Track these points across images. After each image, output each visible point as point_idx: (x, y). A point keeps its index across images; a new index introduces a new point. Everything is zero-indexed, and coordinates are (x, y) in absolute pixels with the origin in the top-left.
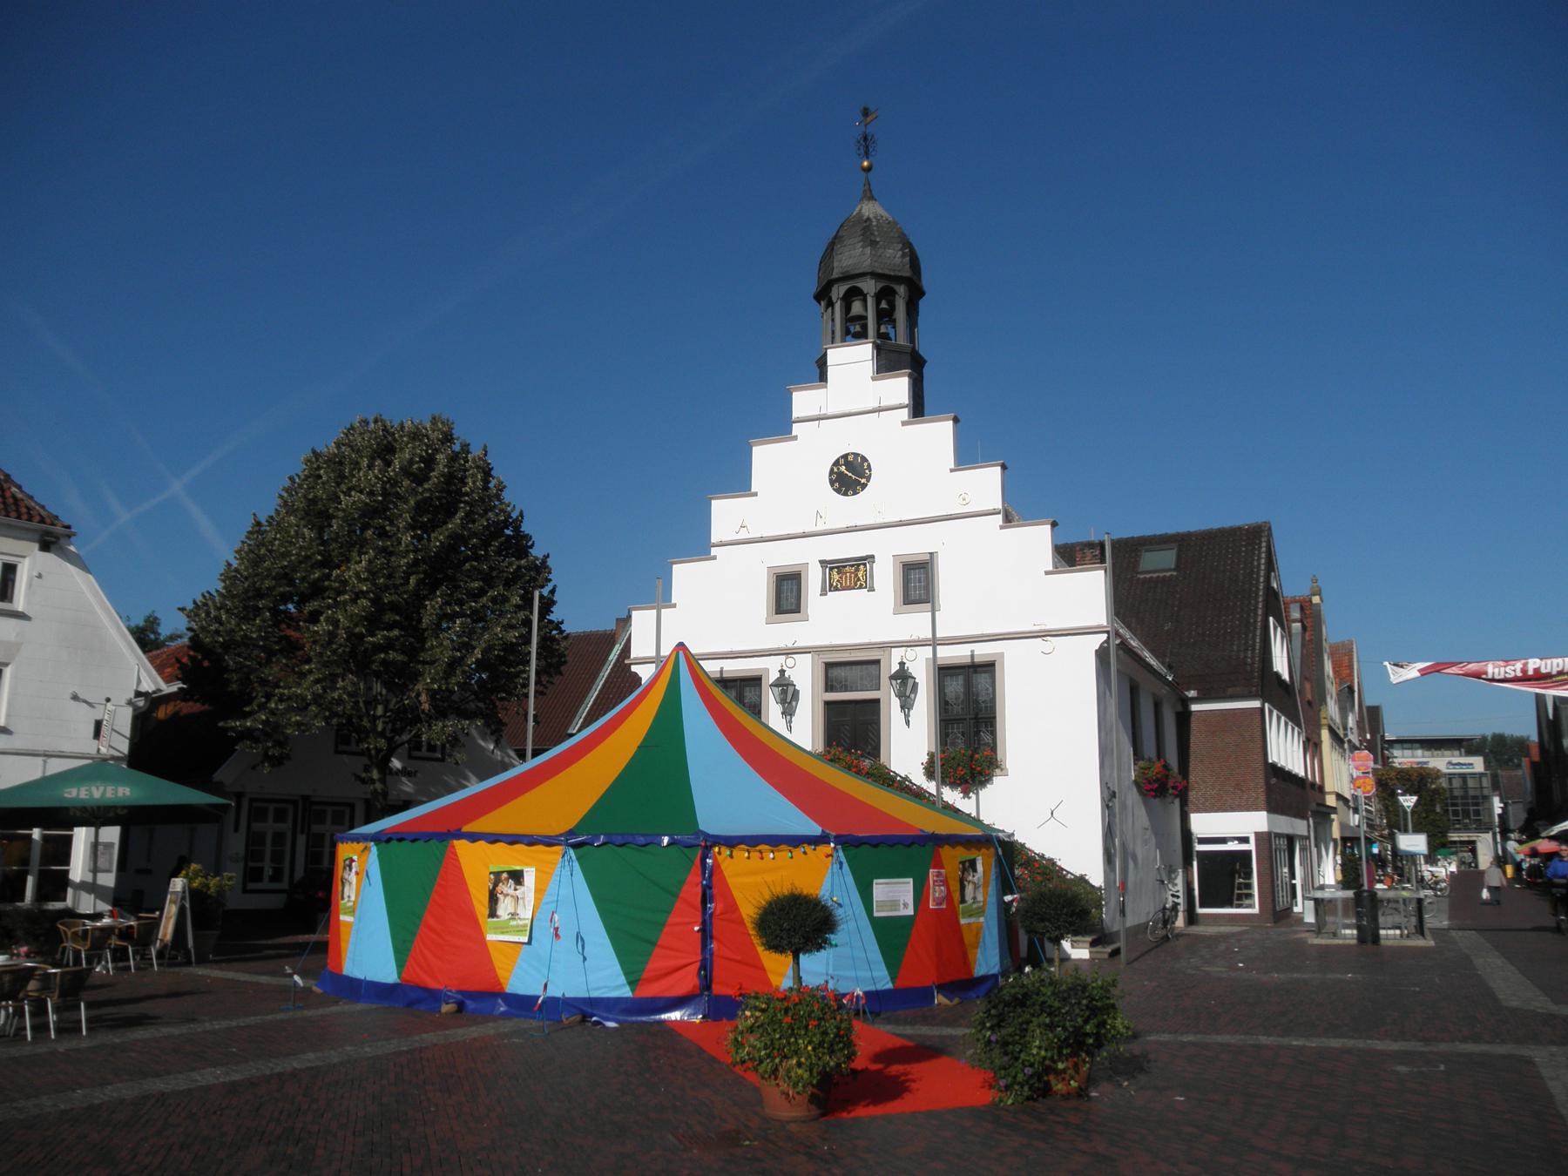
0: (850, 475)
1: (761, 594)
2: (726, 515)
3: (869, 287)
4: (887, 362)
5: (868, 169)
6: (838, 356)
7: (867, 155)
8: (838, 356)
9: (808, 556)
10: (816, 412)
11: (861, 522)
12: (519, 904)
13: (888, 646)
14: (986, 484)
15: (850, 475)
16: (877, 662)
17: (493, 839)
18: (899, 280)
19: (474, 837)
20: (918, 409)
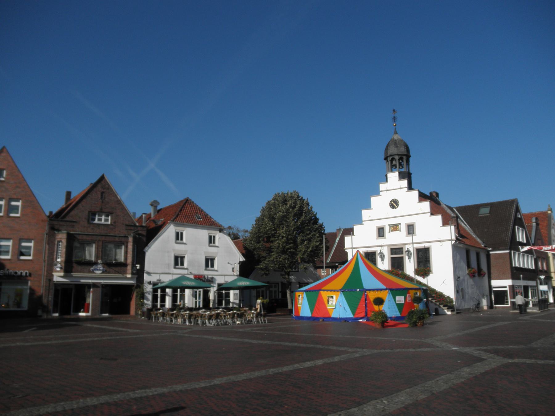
0: (394, 204)
1: (375, 233)
2: (366, 214)
3: (397, 157)
4: (402, 176)
5: (395, 126)
6: (390, 175)
7: (395, 122)
8: (390, 175)
9: (386, 224)
10: (385, 189)
12: (333, 302)
15: (394, 204)
16: (402, 248)
17: (327, 291)
18: (404, 155)
19: (324, 290)
20: (410, 188)
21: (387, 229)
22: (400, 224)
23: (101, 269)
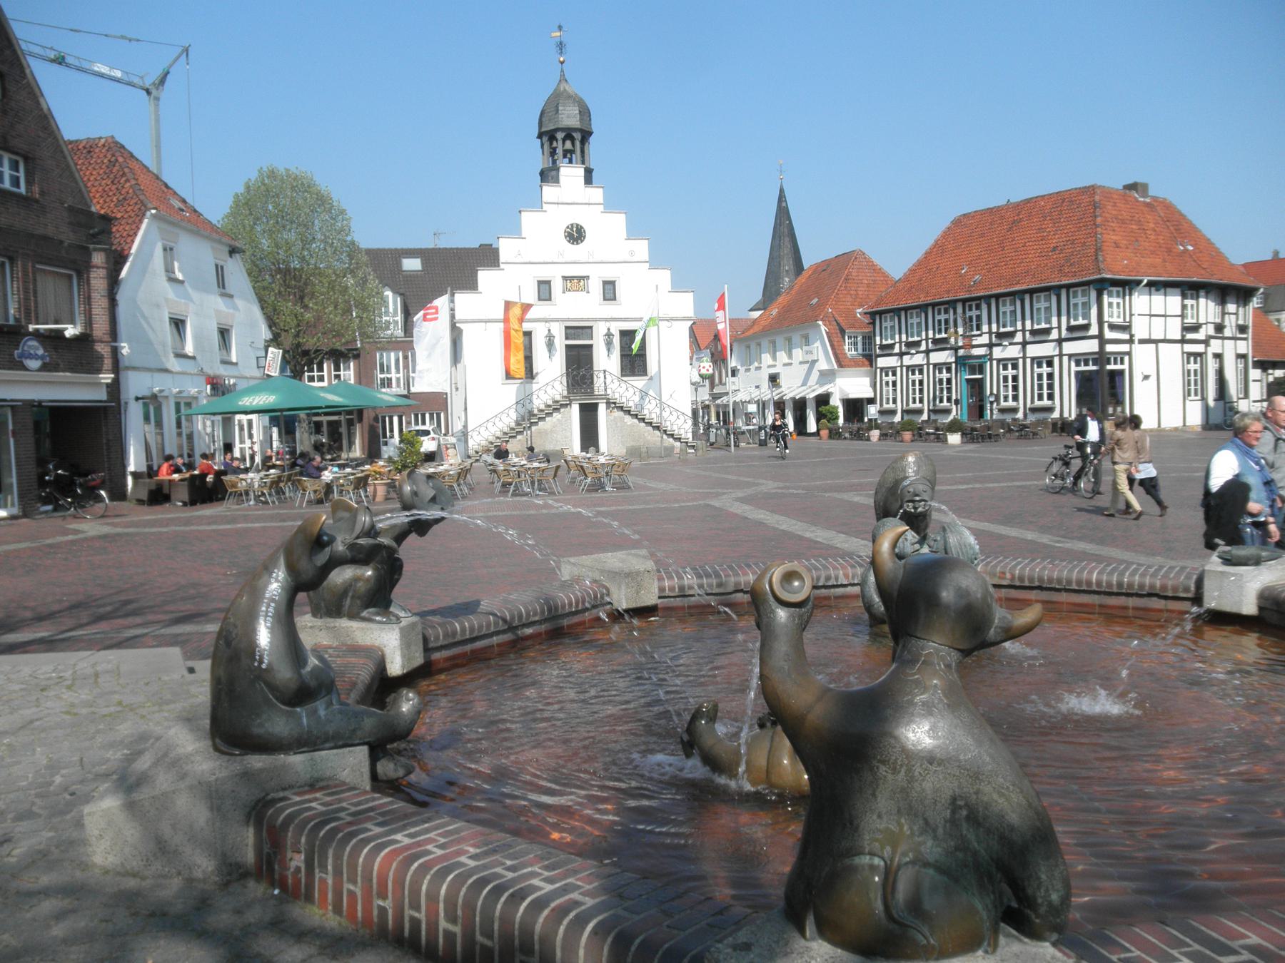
0: (576, 235)
9: (555, 275)
11: (577, 259)
13: (596, 320)
14: (641, 248)
15: (576, 235)
21: (557, 286)
22: (588, 277)
23: (41, 352)
